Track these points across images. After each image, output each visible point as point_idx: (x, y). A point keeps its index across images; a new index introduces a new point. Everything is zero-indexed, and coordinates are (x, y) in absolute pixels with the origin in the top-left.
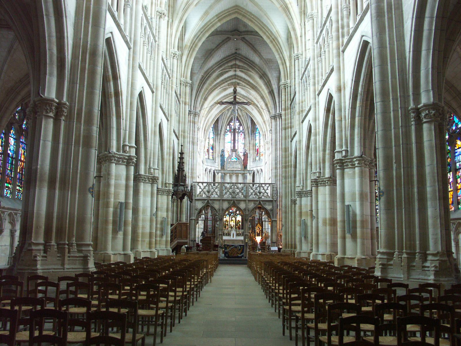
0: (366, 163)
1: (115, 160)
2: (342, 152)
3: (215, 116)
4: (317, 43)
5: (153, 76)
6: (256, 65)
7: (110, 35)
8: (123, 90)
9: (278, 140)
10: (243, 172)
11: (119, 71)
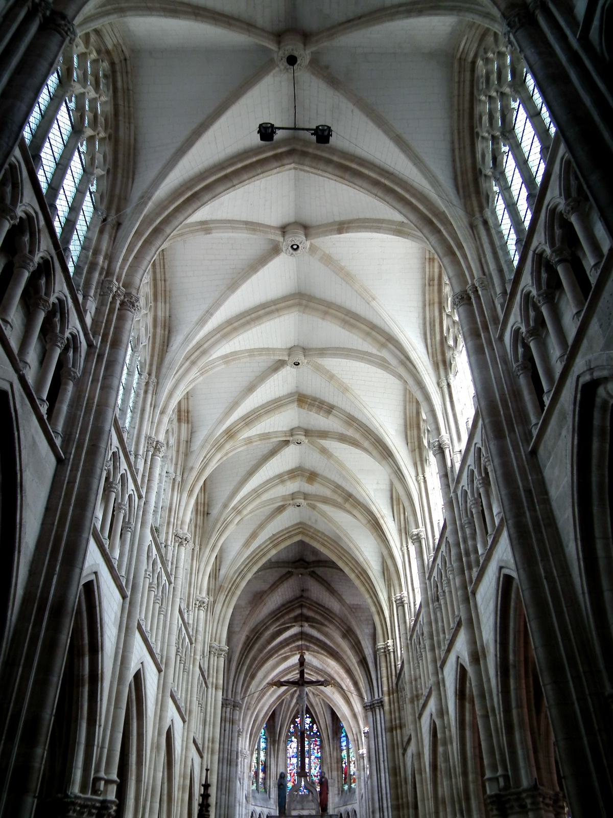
0: (547, 801)
1: (74, 811)
2: (497, 779)
4: (429, 578)
5: (163, 642)
6: (335, 615)
7: (93, 577)
8: (105, 670)
11: (102, 636)
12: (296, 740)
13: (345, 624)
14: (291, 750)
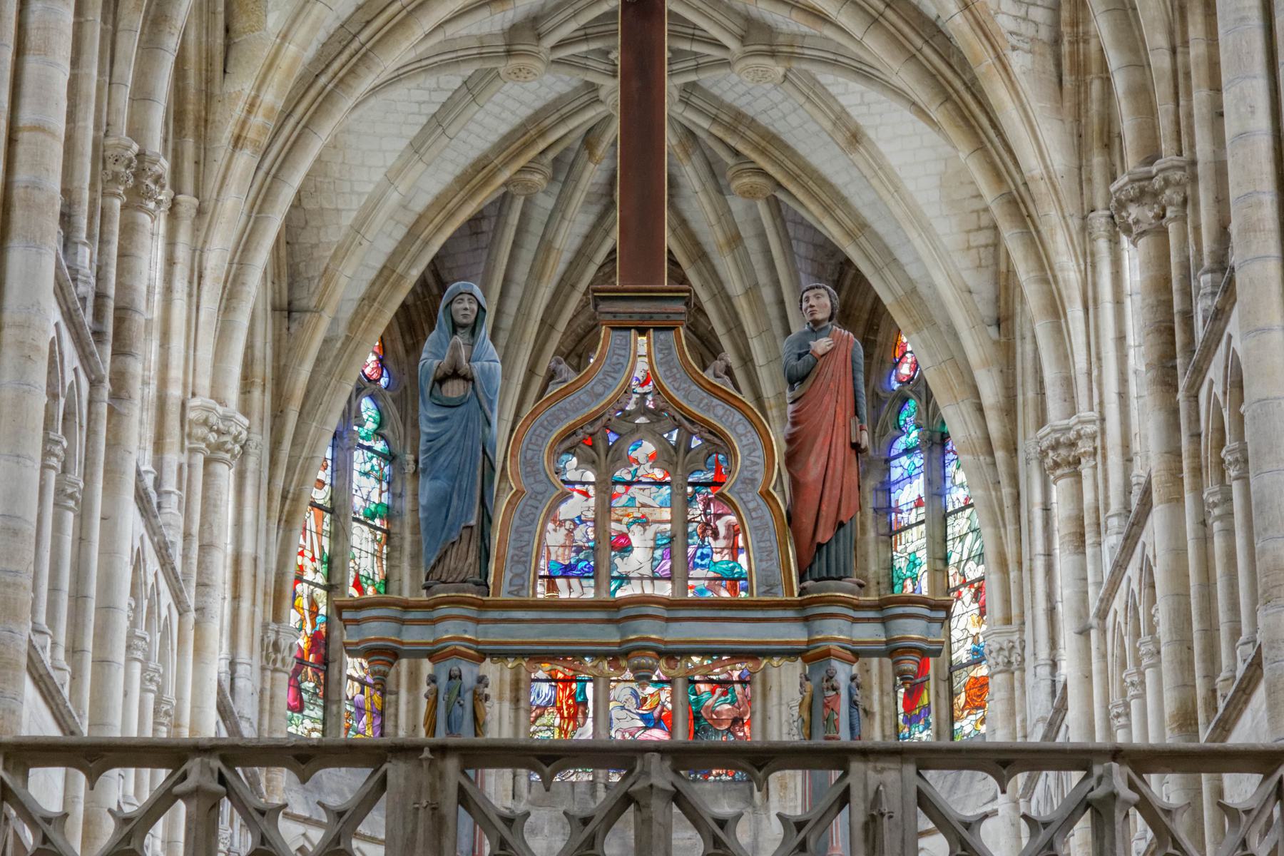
3: (412, 234)
10: (795, 634)
12: (590, 476)
14: (555, 537)
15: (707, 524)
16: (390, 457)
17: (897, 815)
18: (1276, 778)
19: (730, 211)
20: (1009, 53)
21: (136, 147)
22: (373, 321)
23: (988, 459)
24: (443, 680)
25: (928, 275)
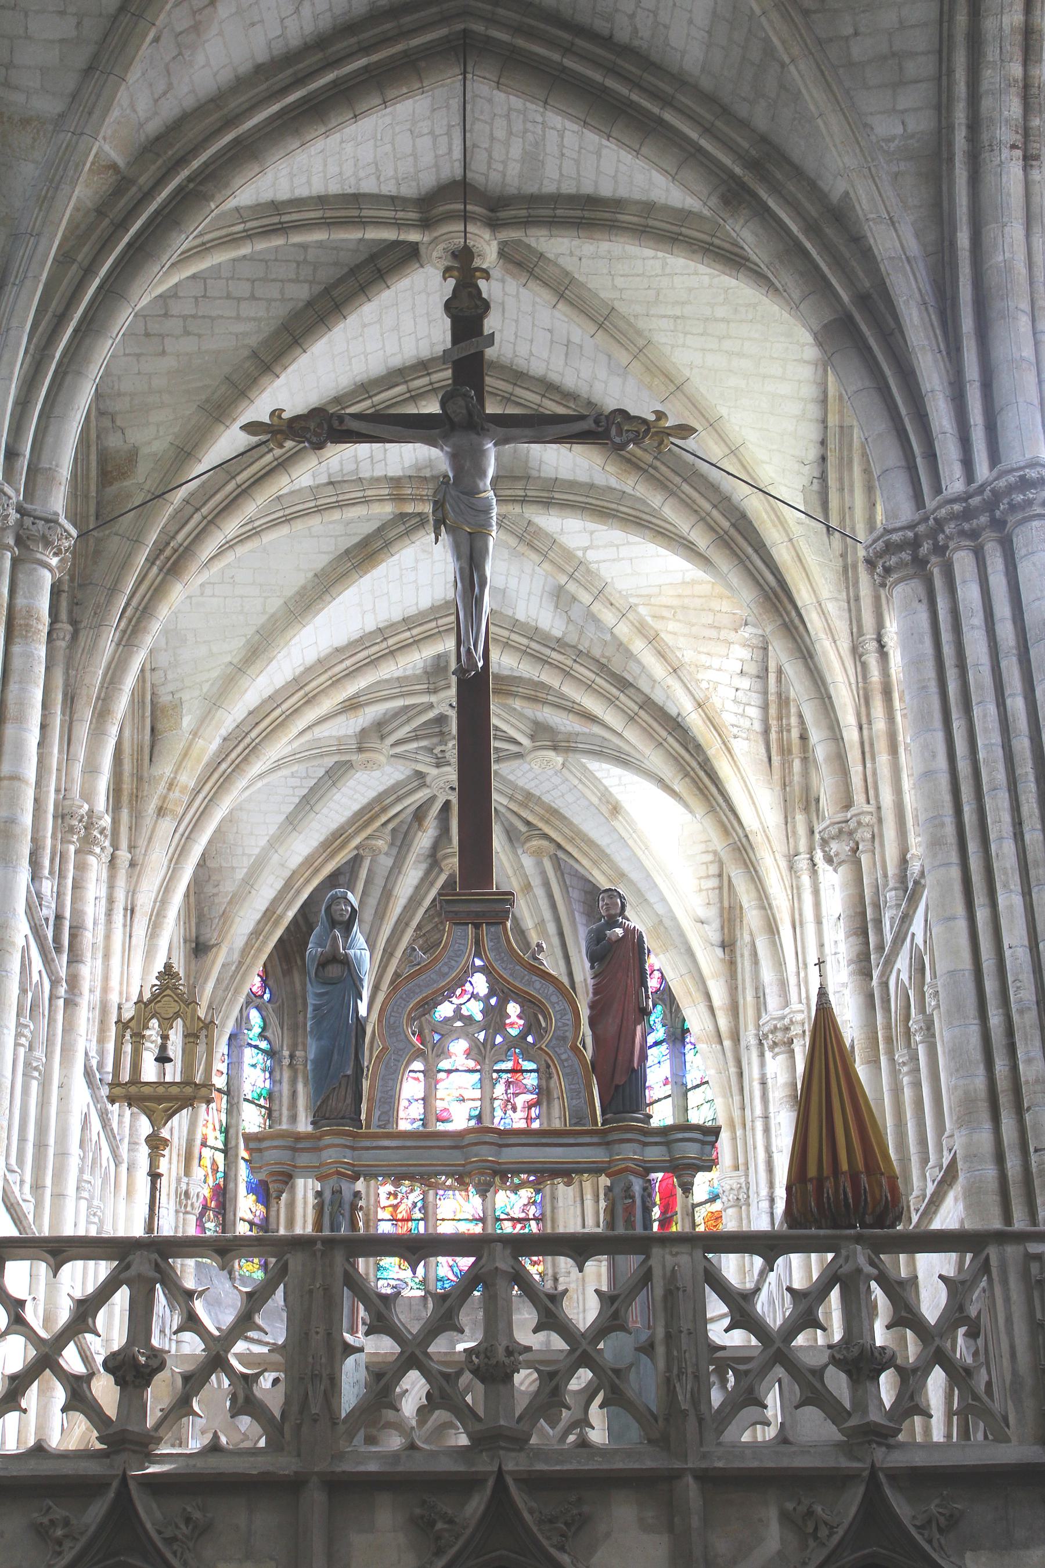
6: (681, 81)
9: (994, 774)
10: (597, 1155)
13: (743, 124)
15: (508, 1101)
16: (271, 1054)
17: (690, 1289)
18: (983, 1256)
19: (522, 866)
20: (732, 740)
21: (86, 807)
22: (259, 950)
23: (719, 1047)
24: (327, 1195)
25: (671, 911)
